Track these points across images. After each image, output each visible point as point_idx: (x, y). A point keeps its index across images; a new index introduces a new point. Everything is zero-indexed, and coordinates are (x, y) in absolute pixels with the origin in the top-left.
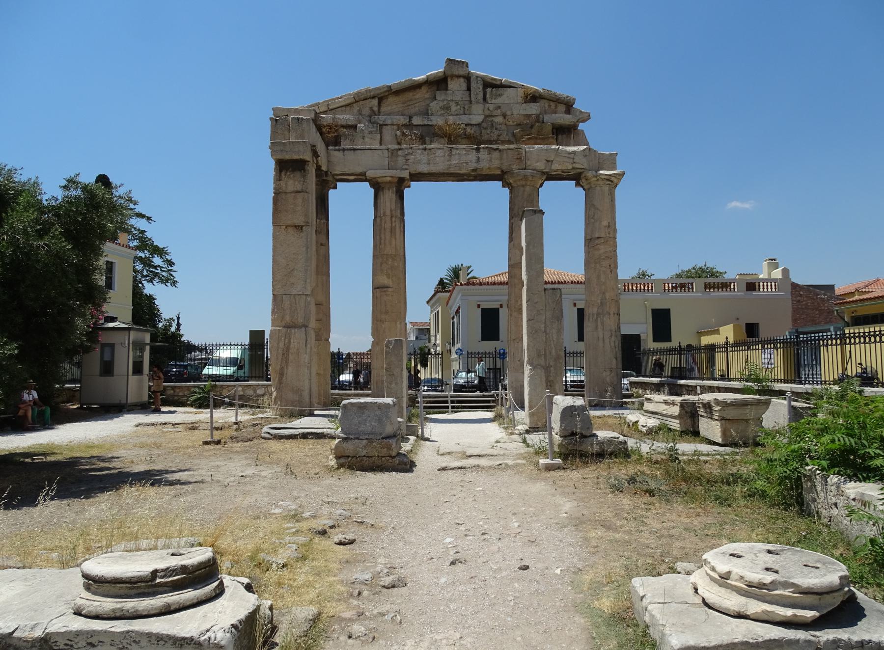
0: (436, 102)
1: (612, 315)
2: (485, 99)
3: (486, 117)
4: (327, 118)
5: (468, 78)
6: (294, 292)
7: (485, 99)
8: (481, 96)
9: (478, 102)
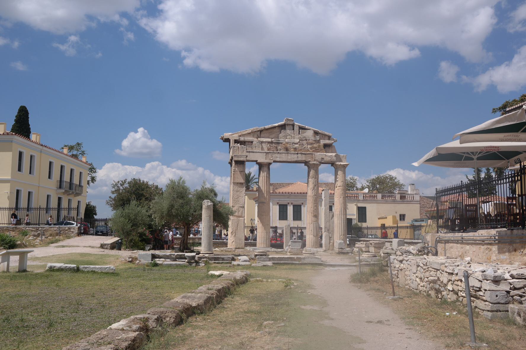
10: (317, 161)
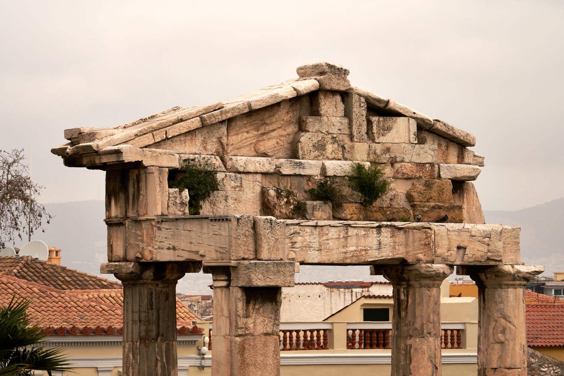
5: (345, 95)
8: (364, 129)
9: (361, 140)
10: (444, 260)
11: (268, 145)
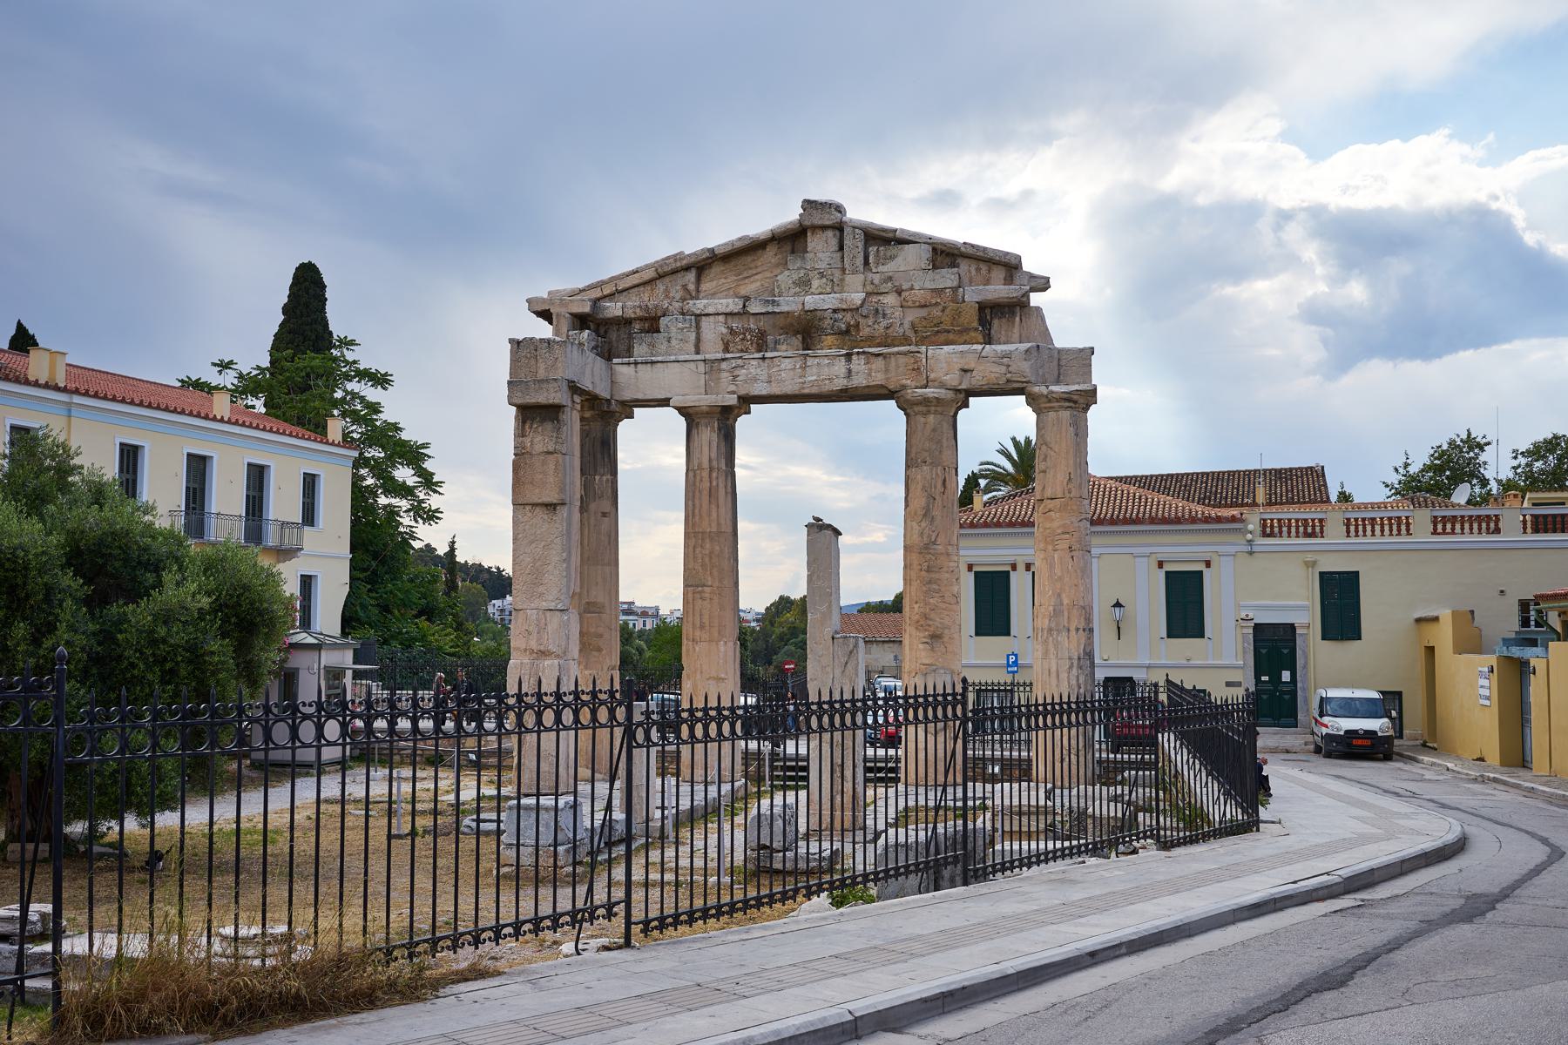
0: (787, 273)
1: (1073, 632)
2: (866, 262)
3: (869, 294)
4: (614, 309)
5: (839, 228)
6: (545, 605)
7: (866, 262)
8: (860, 260)
10: (942, 385)
11: (749, 288)
